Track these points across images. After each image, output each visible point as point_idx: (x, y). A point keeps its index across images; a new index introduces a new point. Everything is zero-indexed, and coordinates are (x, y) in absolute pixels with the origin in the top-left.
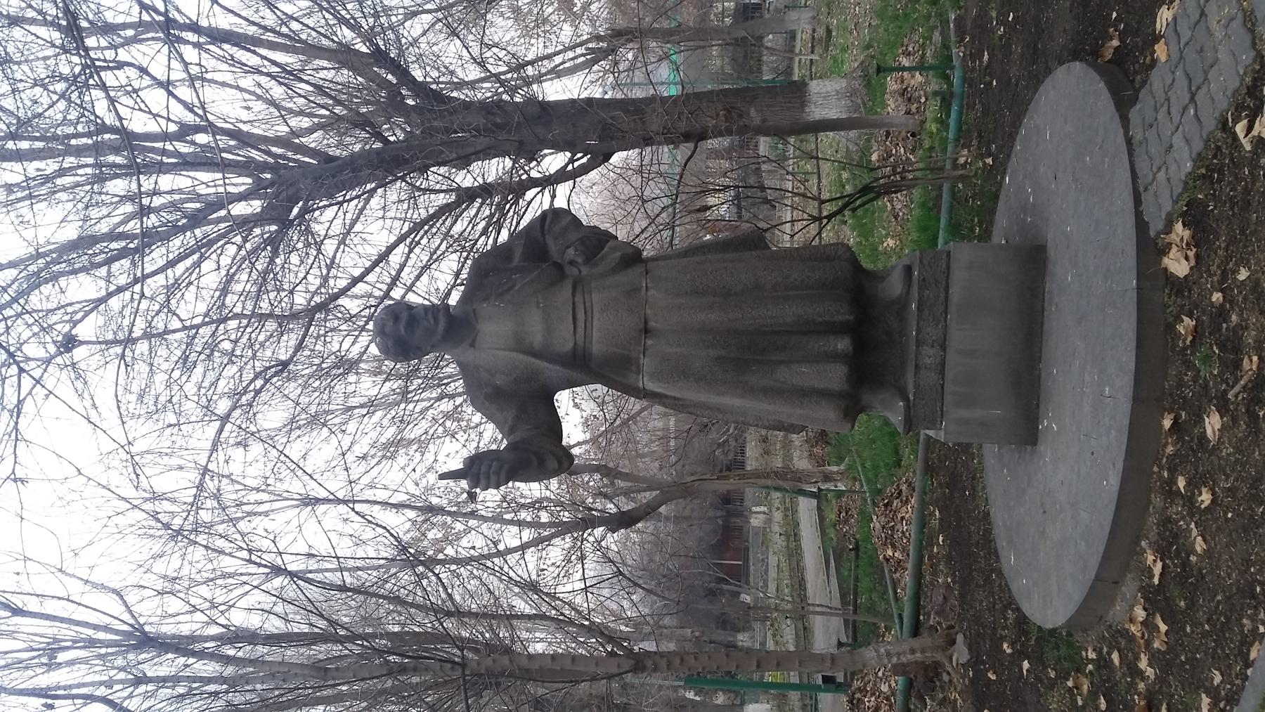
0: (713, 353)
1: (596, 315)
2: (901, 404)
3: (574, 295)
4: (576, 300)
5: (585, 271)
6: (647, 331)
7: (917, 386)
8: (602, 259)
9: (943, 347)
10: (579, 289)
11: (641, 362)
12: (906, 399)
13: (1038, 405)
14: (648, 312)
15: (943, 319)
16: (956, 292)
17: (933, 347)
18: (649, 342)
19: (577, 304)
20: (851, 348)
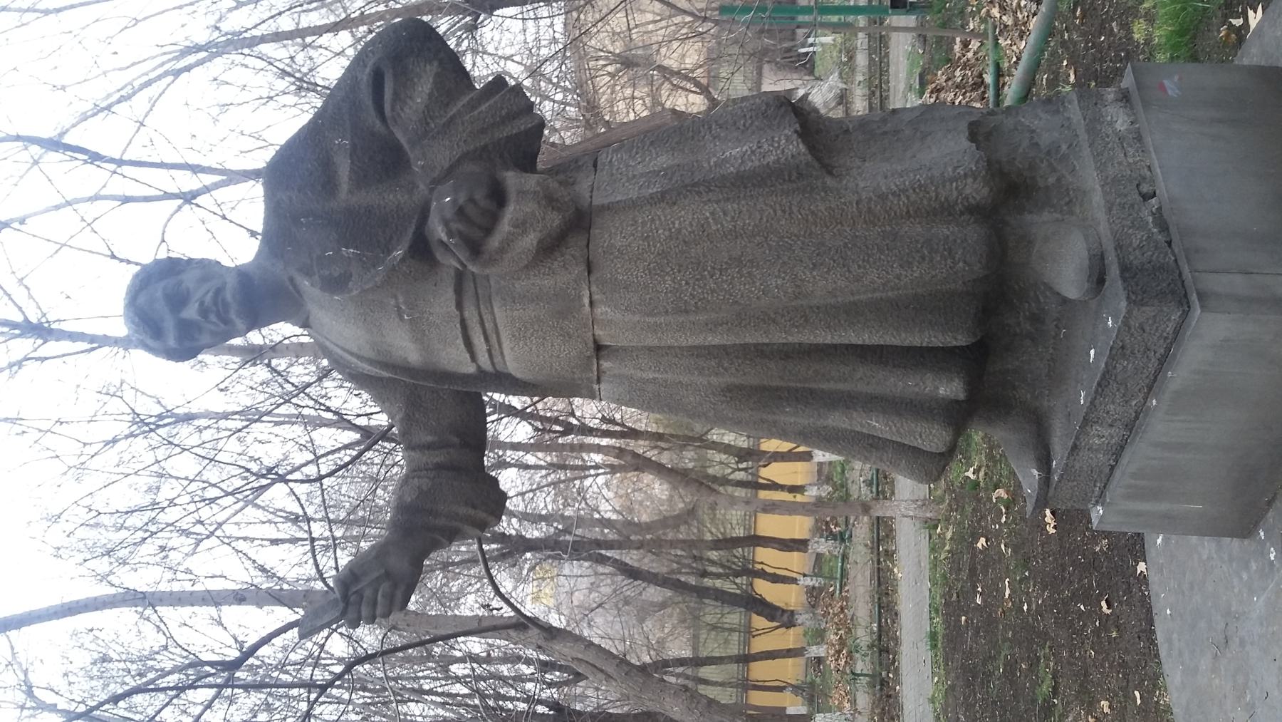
0: (714, 380)
1: (503, 339)
2: (1035, 472)
3: (459, 305)
4: (467, 314)
5: (472, 268)
6: (599, 348)
7: (1066, 468)
8: (502, 250)
9: (1131, 427)
10: (469, 287)
11: (596, 387)
12: (1045, 463)
13: (1270, 503)
14: (598, 332)
15: (1141, 395)
16: (1177, 377)
17: (1111, 426)
18: (606, 364)
19: (469, 322)
20: (962, 396)
